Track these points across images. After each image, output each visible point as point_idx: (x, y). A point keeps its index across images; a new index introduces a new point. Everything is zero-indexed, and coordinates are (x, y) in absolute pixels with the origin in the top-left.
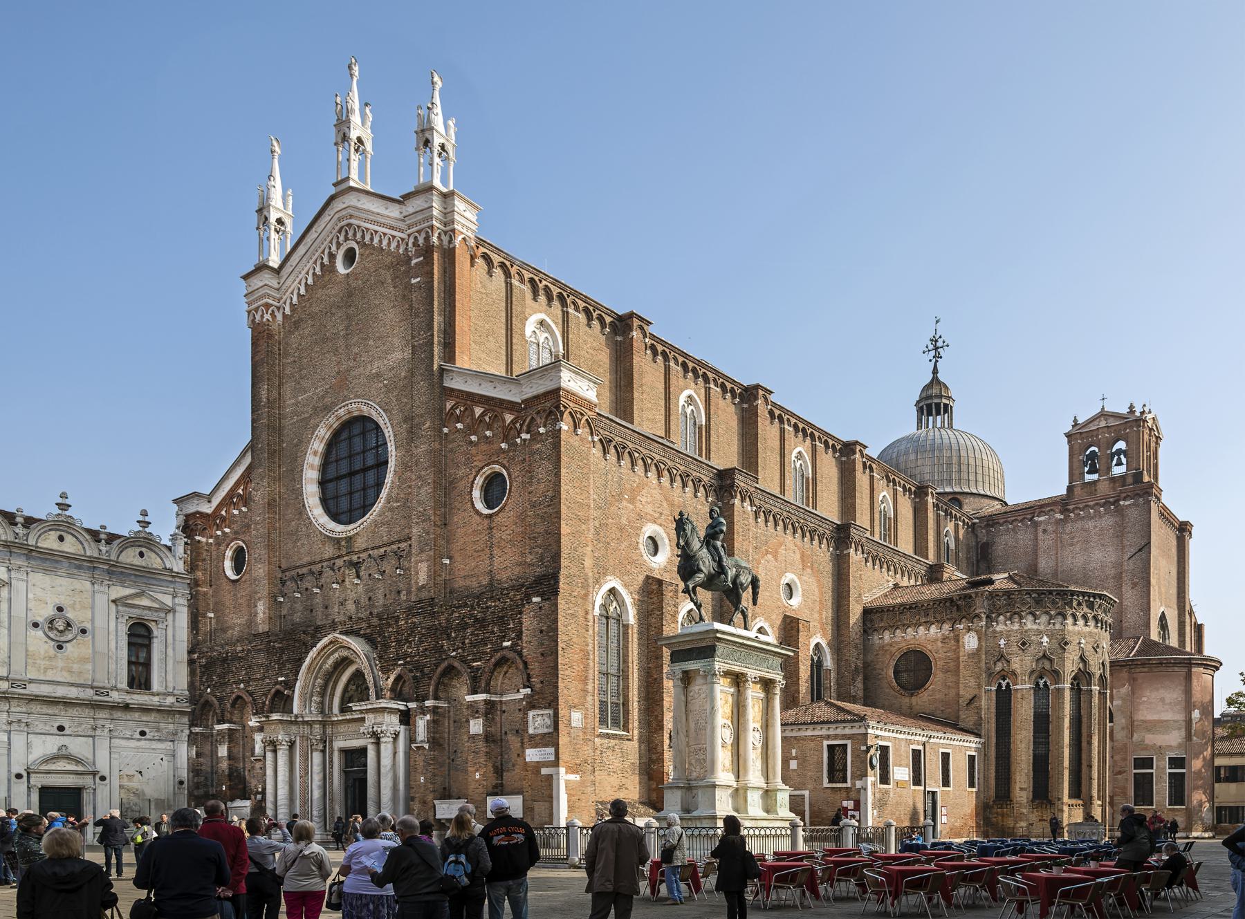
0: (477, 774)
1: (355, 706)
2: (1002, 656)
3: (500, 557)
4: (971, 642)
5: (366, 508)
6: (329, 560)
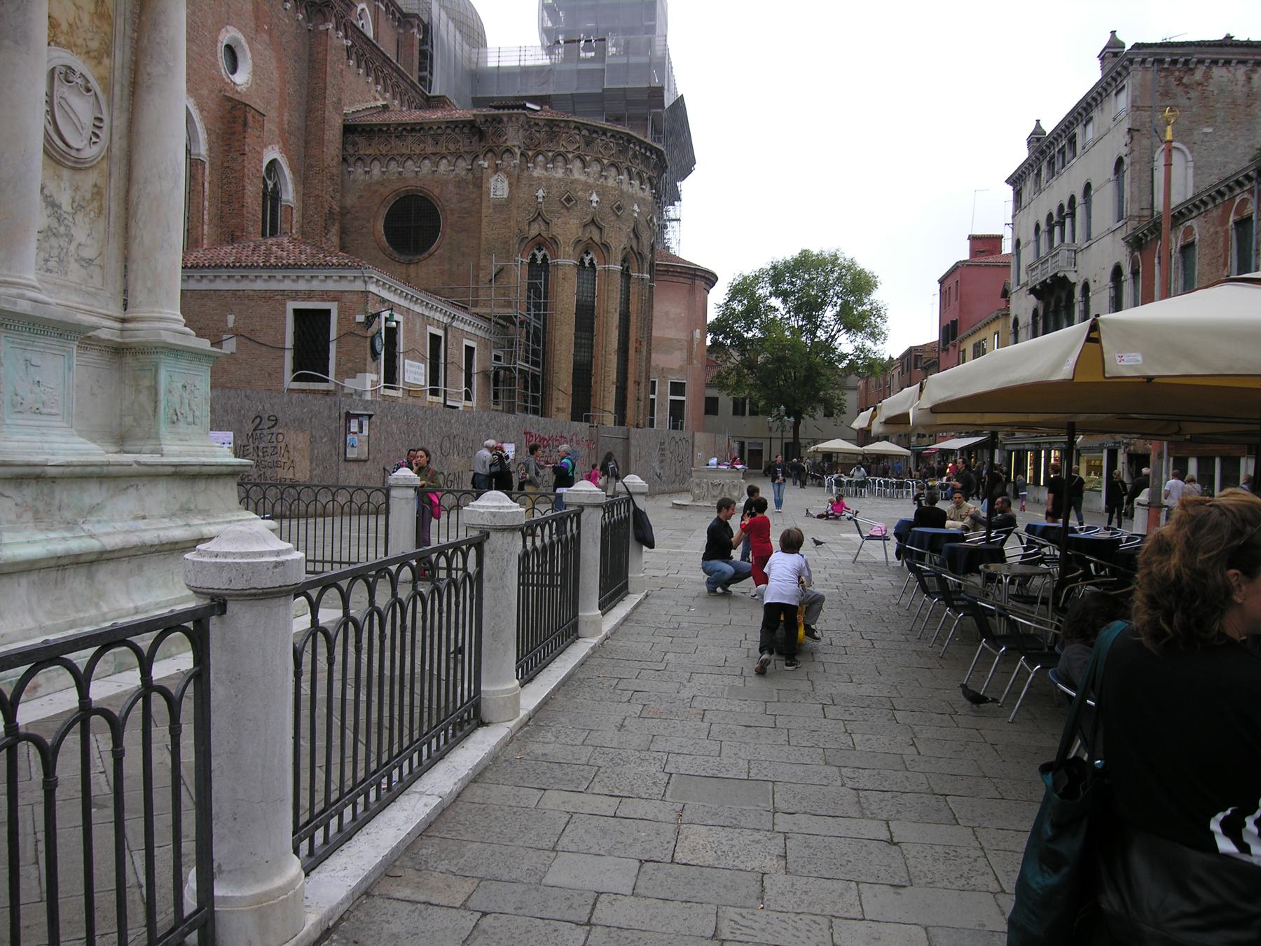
4: (499, 187)
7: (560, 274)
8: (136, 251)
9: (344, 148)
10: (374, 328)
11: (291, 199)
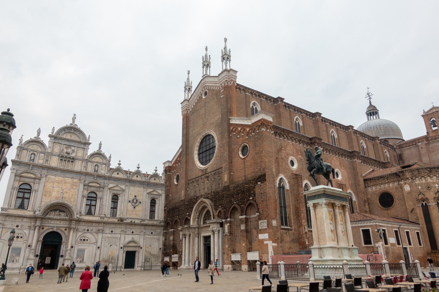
0: (244, 244)
1: (208, 222)
2: (421, 193)
4: (407, 188)
5: (210, 160)
6: (201, 176)
7: (431, 208)
8: (349, 239)
9: (365, 184)
10: (380, 232)
11: (355, 200)
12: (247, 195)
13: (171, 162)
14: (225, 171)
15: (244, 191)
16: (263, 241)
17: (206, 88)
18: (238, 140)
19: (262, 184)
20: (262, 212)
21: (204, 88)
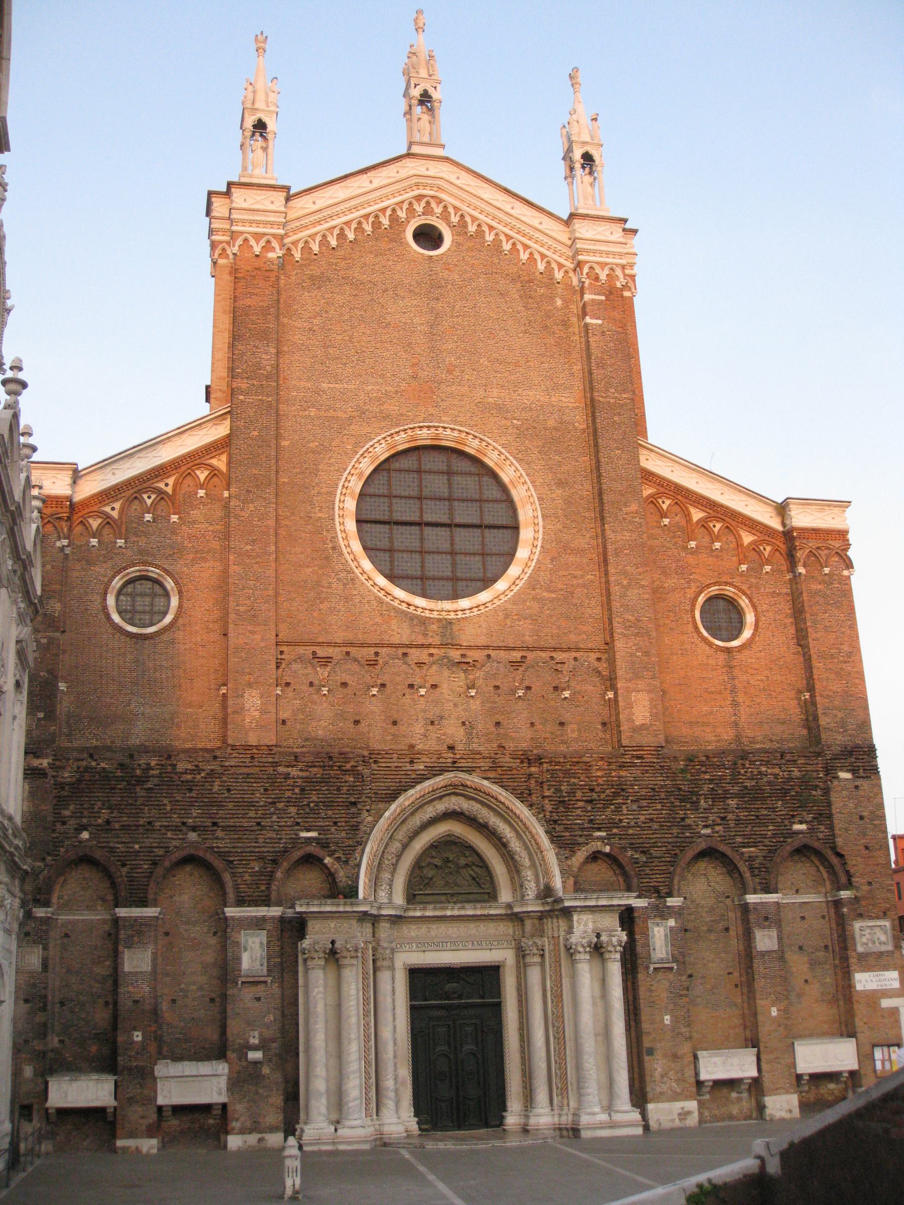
3: (750, 707)
12: (774, 809)
13: (76, 475)
14: (637, 676)
15: (758, 789)
16: (874, 997)
17: (438, 210)
18: (691, 560)
19: (864, 784)
20: (866, 888)
21: (423, 204)
